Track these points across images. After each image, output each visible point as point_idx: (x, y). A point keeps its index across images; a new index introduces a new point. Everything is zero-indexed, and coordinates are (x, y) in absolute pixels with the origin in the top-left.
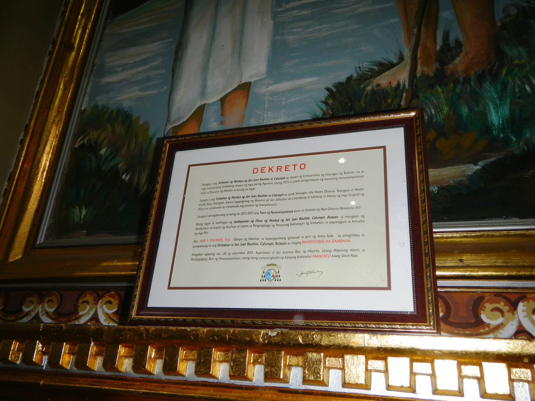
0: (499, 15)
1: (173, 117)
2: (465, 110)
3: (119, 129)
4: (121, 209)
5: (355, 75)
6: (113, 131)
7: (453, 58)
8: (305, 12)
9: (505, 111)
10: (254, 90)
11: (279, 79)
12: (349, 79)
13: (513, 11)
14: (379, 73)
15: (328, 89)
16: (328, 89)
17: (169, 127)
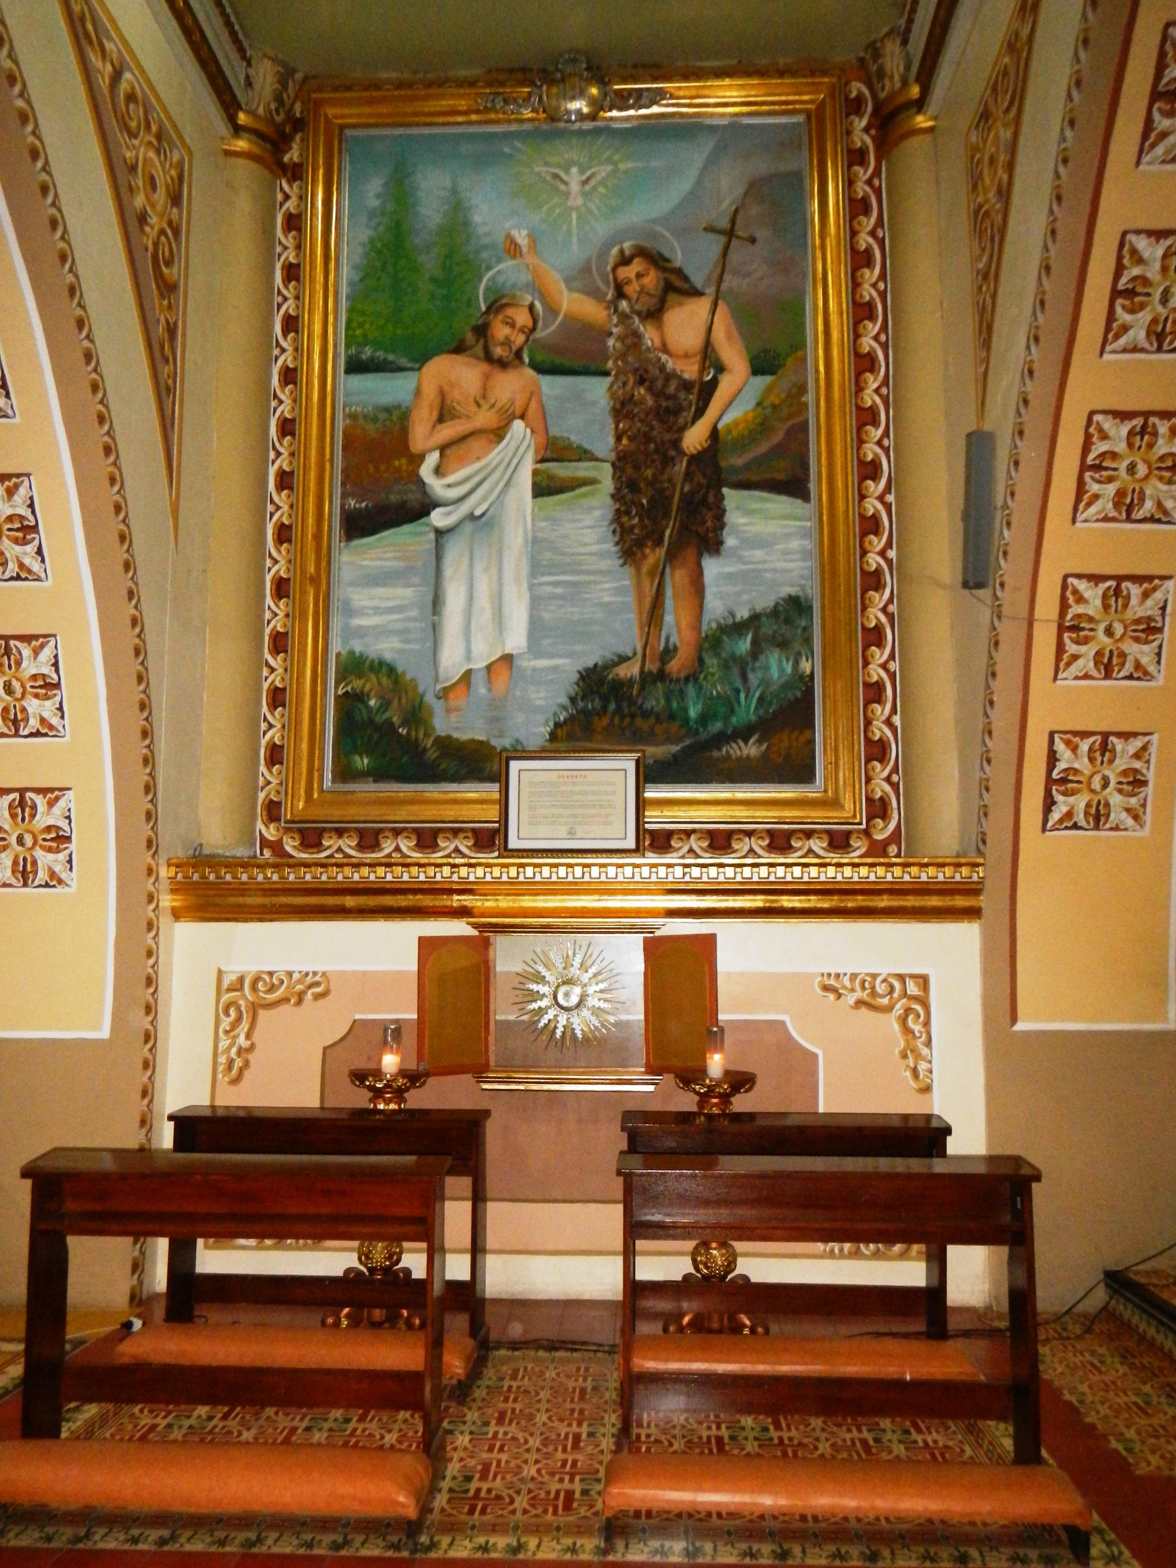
0: (705, 627)
1: (441, 679)
2: (675, 705)
3: (385, 681)
4: (403, 761)
5: (600, 663)
6: (379, 683)
7: (669, 662)
8: (559, 590)
9: (699, 707)
10: (518, 662)
11: (539, 655)
12: (596, 665)
13: (714, 625)
14: (617, 664)
15: (579, 672)
16: (579, 672)
17: (439, 687)
